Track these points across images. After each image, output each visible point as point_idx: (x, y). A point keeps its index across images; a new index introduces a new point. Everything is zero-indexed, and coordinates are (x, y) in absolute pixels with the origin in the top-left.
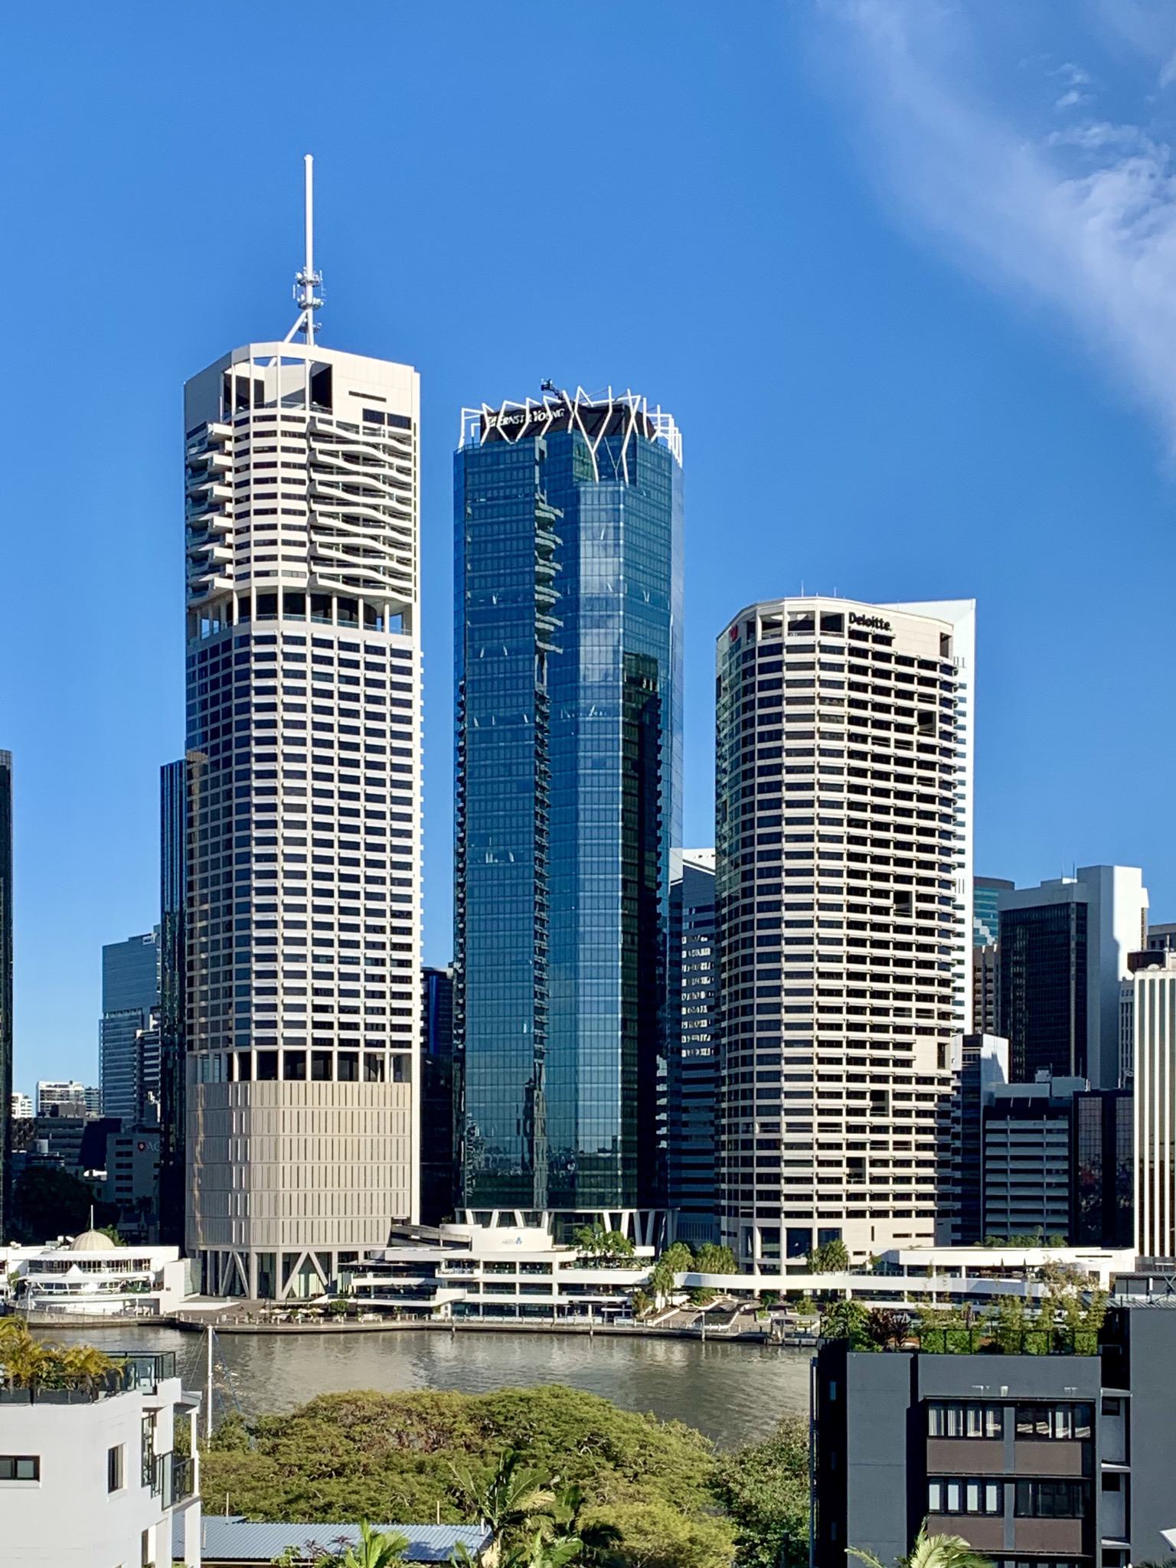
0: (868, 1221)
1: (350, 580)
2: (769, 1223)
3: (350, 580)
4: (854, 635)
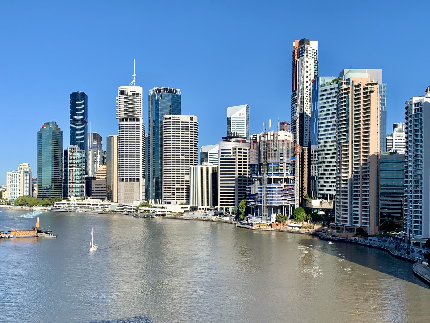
0: (176, 201)
1: (129, 116)
2: (165, 201)
3: (129, 116)
4: (172, 119)
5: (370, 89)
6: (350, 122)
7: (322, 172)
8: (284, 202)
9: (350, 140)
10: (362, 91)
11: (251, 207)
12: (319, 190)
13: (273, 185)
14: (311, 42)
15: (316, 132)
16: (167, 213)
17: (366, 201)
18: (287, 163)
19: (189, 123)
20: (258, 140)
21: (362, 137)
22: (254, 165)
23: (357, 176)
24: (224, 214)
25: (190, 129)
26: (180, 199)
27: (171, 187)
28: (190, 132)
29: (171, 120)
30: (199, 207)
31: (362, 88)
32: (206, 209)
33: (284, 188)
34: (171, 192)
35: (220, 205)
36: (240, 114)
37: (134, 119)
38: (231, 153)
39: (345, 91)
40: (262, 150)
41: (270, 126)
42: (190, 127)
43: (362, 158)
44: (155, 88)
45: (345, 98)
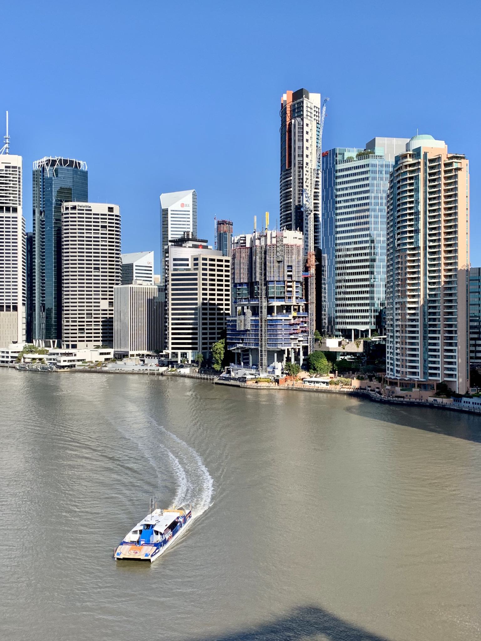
0: (85, 343)
2: (67, 343)
4: (79, 210)
5: (455, 166)
6: (421, 216)
7: (342, 296)
8: (293, 342)
9: (421, 244)
10: (443, 168)
11: (236, 351)
12: (338, 323)
13: (275, 316)
14: (311, 95)
15: (331, 234)
16: (77, 363)
17: (450, 341)
18: (297, 282)
19: (107, 217)
20: (248, 245)
21: (443, 240)
22: (241, 284)
23: (434, 301)
24: (179, 362)
25: (109, 227)
26: (93, 339)
27: (78, 320)
28: (109, 230)
29: (77, 211)
30: (131, 353)
31: (442, 163)
32: (143, 355)
33: (292, 321)
34: (78, 327)
35: (173, 348)
36: (183, 205)
37: (8, 209)
38: (190, 265)
39: (411, 169)
40: (258, 260)
41: (267, 222)
42: (109, 223)
43: (443, 273)
44: (45, 159)
45: (411, 178)
